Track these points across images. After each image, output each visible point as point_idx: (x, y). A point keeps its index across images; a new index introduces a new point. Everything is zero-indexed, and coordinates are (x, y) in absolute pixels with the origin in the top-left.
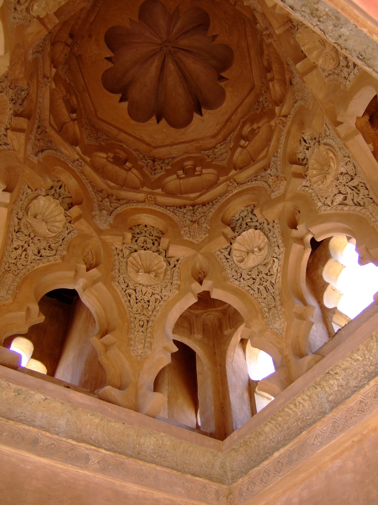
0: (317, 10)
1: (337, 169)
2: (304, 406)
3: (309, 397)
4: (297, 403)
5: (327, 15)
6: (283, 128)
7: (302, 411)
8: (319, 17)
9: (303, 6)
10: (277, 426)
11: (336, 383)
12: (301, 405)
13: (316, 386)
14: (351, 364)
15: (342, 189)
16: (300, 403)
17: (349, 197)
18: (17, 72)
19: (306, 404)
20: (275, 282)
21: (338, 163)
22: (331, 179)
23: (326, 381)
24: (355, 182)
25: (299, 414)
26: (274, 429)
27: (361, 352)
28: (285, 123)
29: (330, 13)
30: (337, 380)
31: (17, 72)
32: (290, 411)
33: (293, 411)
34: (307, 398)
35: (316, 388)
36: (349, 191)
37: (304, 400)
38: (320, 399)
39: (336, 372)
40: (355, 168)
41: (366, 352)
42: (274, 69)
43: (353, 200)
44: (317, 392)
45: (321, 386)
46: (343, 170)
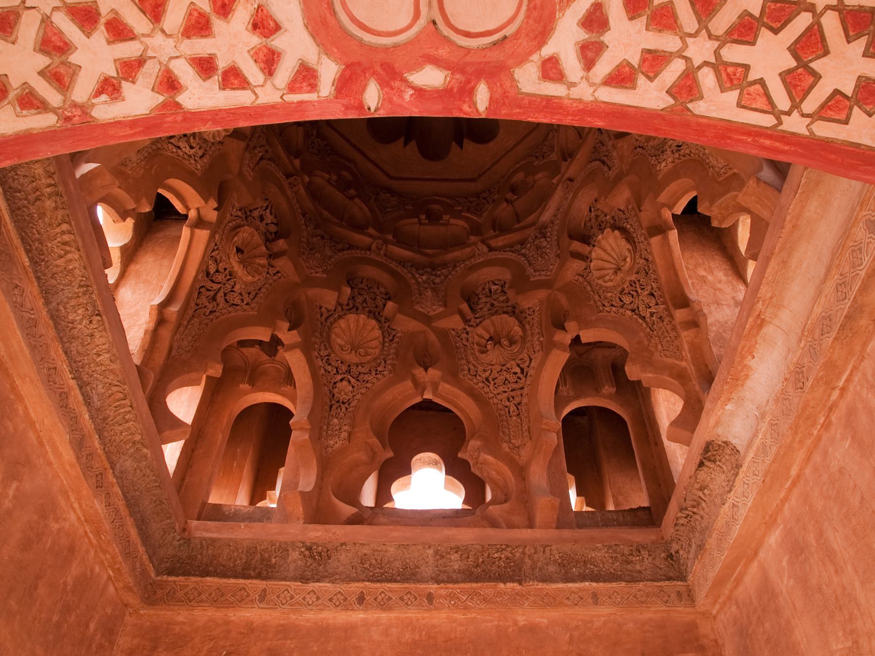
0: (457, 552)
1: (241, 279)
2: (61, 257)
3: (72, 269)
4: (68, 248)
5: (449, 553)
6: (289, 181)
7: (52, 251)
8: (451, 549)
9: (467, 548)
10: (38, 193)
11: (78, 318)
12: (63, 252)
13: (85, 289)
14: (98, 346)
15: (220, 278)
16: (67, 252)
17: (209, 285)
18: (625, 147)
19: (61, 262)
20: (169, 143)
21: (245, 283)
22: (236, 268)
23: (86, 304)
24: (220, 297)
25: (50, 245)
26: (34, 184)
27: (107, 362)
28: (292, 188)
29: (448, 556)
30: (82, 320)
31: (625, 147)
32: (58, 230)
33: (57, 234)
34: (71, 267)
35: (80, 286)
36: (216, 287)
37: (71, 260)
38: (62, 287)
39: (94, 322)
40: (233, 304)
41: (103, 368)
42: (338, 192)
43: (203, 287)
44: (74, 284)
45: (80, 294)
46: (237, 287)
